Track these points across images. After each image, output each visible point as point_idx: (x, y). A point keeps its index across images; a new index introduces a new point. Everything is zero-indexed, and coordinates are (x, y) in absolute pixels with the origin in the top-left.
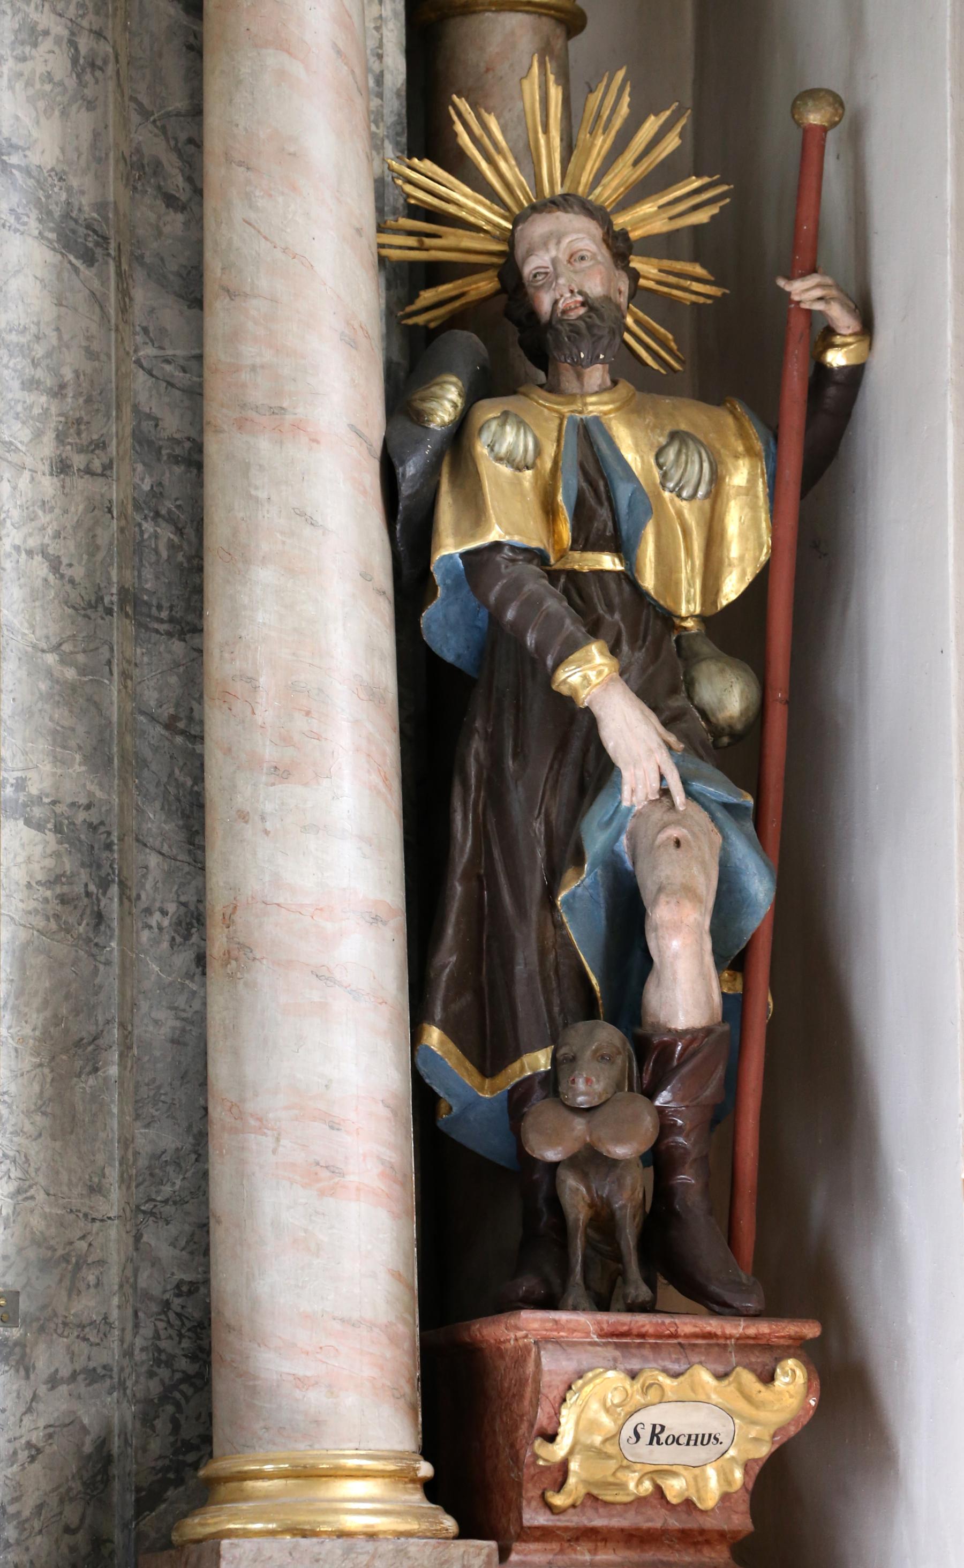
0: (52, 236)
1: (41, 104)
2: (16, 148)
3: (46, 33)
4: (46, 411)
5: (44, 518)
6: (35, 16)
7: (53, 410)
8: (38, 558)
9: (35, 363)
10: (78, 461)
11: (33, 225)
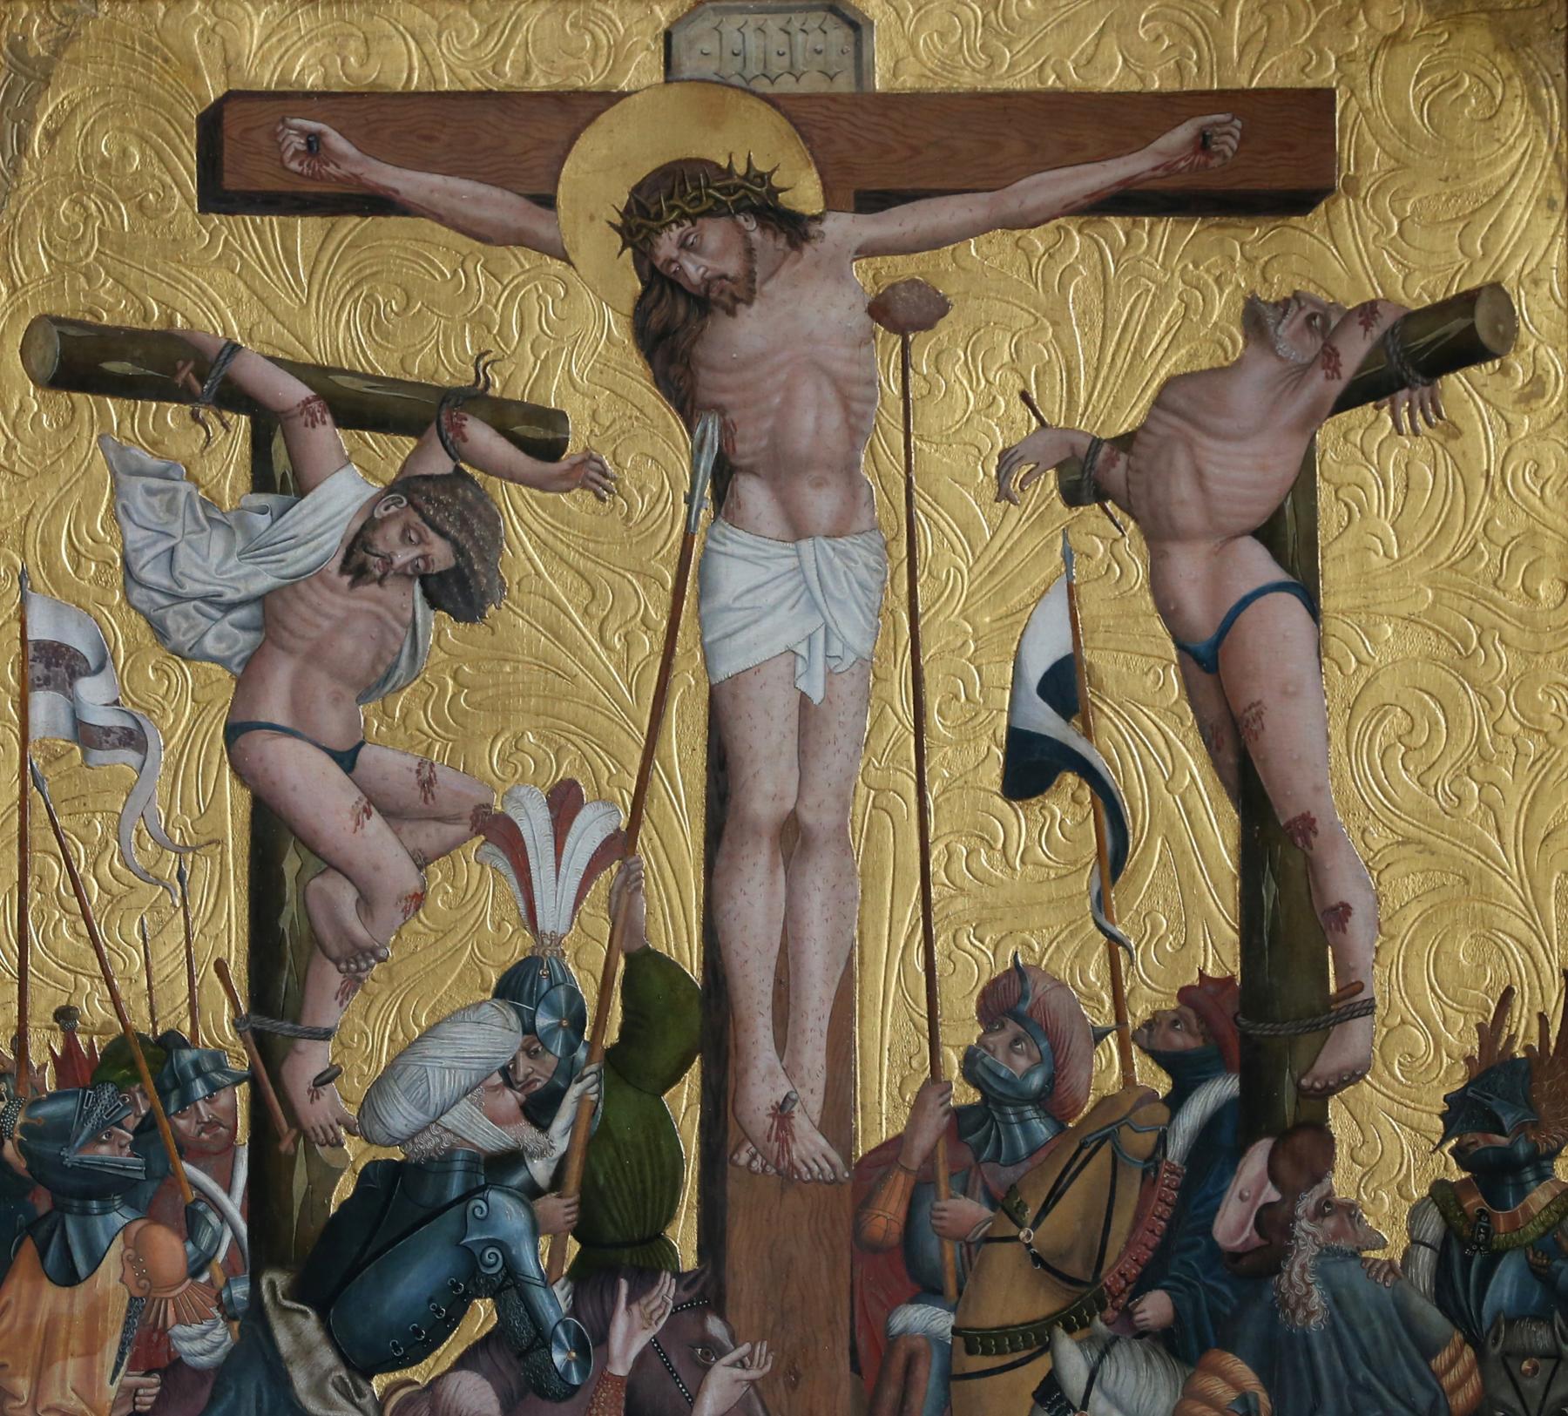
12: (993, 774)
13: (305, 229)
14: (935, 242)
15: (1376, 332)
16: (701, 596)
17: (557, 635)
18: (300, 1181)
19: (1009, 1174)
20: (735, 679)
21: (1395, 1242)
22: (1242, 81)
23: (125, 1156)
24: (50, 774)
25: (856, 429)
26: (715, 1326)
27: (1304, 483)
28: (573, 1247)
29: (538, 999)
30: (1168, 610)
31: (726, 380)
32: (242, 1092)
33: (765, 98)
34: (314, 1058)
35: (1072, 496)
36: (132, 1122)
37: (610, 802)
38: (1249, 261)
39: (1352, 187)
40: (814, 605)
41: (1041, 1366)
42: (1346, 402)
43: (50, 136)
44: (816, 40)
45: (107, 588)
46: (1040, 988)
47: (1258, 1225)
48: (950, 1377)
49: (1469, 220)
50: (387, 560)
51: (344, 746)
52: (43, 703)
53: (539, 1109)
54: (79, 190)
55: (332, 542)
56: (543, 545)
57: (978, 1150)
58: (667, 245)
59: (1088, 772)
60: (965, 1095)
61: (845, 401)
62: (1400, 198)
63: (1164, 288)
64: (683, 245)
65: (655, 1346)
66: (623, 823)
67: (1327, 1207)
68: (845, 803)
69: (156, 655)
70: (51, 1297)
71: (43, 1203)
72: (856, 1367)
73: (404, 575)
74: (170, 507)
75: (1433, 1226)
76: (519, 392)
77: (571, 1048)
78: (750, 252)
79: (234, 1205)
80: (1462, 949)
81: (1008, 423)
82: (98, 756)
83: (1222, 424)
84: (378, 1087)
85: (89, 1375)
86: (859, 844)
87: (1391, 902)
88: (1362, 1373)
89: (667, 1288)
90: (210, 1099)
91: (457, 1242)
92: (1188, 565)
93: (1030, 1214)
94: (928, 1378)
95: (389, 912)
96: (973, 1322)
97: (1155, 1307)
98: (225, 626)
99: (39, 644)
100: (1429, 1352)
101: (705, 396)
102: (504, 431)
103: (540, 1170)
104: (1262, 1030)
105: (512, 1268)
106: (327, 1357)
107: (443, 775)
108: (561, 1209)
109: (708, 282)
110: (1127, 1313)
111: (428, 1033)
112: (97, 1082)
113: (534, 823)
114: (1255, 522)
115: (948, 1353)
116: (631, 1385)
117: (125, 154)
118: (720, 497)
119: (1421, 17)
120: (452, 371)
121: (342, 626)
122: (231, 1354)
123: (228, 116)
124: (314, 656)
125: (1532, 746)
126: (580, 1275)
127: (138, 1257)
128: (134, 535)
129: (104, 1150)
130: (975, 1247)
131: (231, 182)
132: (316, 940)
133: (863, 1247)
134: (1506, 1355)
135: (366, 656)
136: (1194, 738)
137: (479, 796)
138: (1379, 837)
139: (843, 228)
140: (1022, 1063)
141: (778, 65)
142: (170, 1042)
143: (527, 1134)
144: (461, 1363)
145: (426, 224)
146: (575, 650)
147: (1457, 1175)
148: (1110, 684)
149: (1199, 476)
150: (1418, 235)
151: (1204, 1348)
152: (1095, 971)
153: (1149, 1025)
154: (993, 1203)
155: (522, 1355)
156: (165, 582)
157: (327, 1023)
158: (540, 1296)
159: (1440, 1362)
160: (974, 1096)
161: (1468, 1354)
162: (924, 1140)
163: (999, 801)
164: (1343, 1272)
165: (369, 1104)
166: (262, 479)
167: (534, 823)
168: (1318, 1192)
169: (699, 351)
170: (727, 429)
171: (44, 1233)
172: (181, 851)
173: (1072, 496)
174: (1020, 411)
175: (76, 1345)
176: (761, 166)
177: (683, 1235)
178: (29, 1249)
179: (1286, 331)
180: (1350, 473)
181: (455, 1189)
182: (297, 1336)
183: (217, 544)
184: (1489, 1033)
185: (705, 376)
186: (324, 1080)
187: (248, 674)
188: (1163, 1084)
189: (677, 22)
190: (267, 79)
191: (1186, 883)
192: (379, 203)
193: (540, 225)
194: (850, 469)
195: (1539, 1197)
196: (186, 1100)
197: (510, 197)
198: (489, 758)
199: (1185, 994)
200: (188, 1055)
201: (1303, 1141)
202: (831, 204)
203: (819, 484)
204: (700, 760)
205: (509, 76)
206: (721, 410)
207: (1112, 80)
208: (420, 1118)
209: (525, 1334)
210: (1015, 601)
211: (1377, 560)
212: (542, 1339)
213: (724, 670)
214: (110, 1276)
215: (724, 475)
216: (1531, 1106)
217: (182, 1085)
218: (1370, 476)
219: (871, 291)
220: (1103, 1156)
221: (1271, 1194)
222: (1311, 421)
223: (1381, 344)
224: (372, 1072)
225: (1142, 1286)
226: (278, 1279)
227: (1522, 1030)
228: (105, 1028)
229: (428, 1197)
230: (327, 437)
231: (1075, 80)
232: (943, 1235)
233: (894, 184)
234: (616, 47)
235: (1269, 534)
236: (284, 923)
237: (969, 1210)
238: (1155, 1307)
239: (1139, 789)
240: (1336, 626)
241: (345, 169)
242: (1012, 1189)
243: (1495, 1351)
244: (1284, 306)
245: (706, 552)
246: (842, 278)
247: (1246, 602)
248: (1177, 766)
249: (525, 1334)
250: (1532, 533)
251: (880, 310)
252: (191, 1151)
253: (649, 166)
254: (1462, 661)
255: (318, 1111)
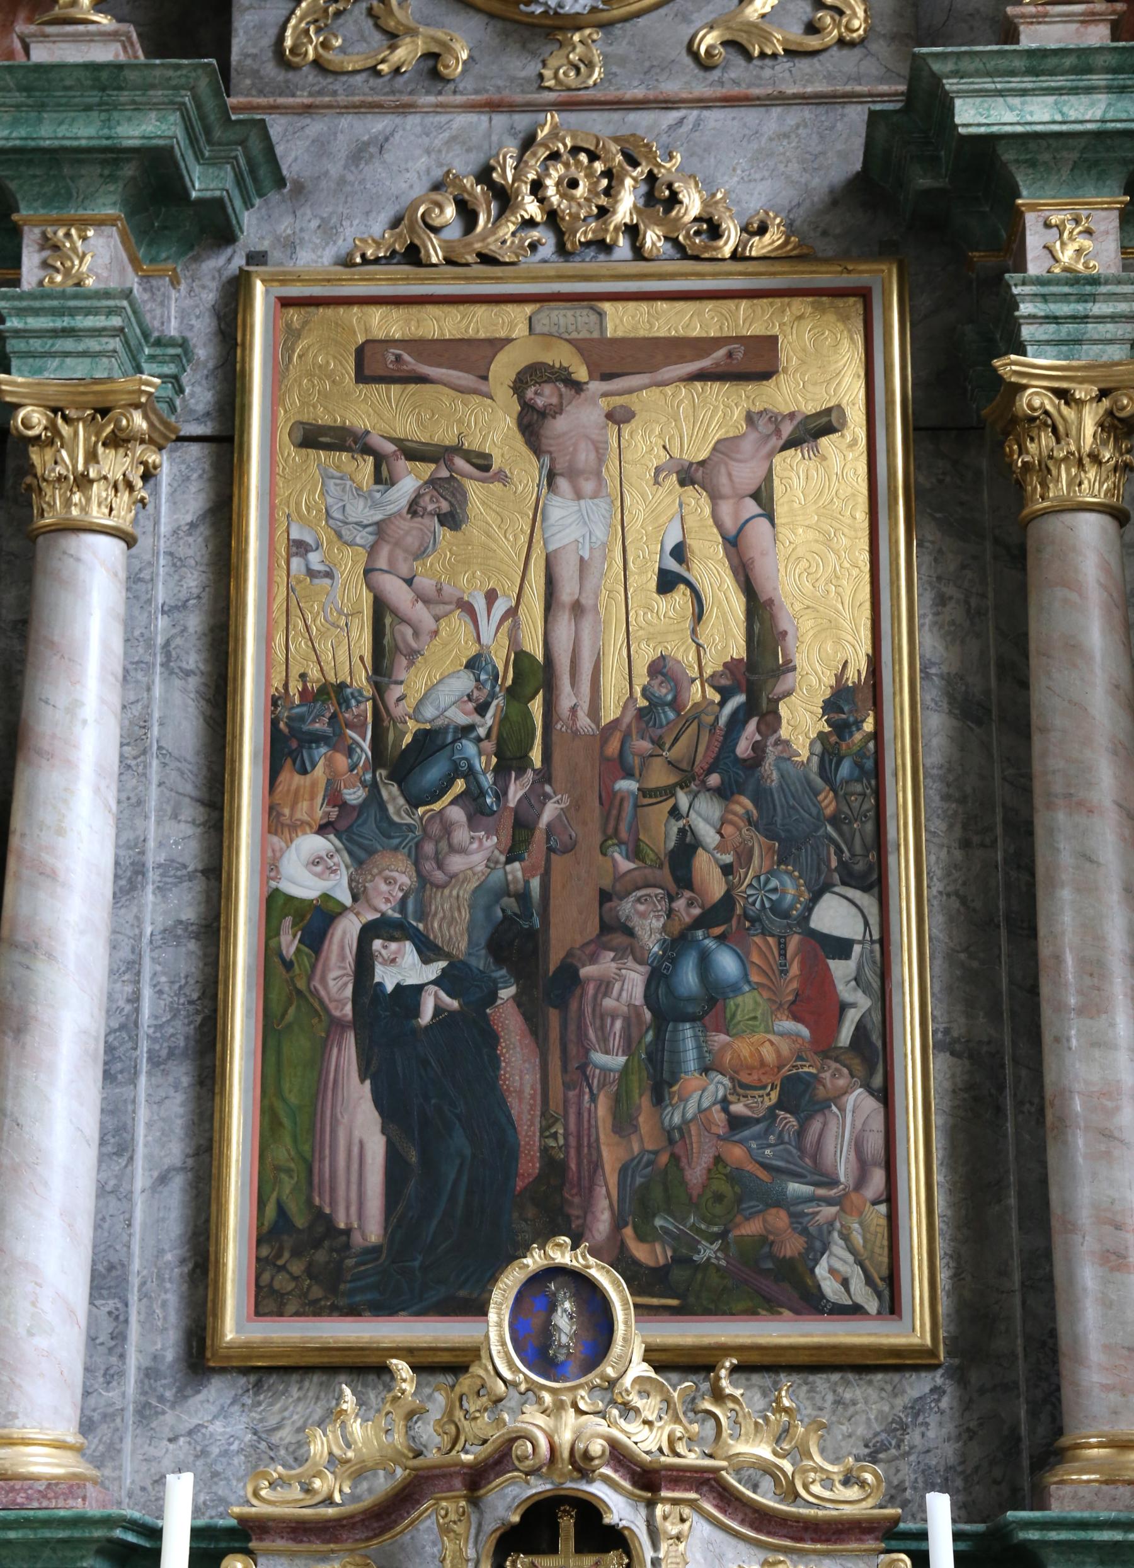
0: (957, 712)
1: (949, 638)
2: (934, 664)
3: (951, 598)
4: (956, 813)
5: (956, 874)
6: (944, 589)
7: (960, 811)
8: (953, 898)
9: (948, 785)
10: (976, 839)
11: (945, 706)
12: (653, 584)
13: (395, 389)
14: (630, 391)
15: (795, 422)
16: (543, 520)
17: (488, 536)
18: (391, 736)
19: (659, 732)
20: (555, 551)
21: (804, 754)
22: (744, 333)
23: (325, 727)
24: (298, 588)
25: (601, 459)
26: (548, 788)
27: (769, 478)
28: (494, 760)
29: (481, 669)
30: (718, 524)
31: (552, 442)
32: (369, 704)
33: (566, 340)
34: (396, 691)
35: (682, 483)
36: (328, 715)
37: (509, 596)
38: (748, 397)
39: (785, 370)
40: (585, 523)
41: (671, 802)
42: (784, 448)
43: (300, 357)
44: (585, 319)
45: (320, 520)
46: (670, 664)
47: (753, 749)
48: (637, 806)
49: (828, 382)
50: (425, 509)
51: (408, 577)
52: (296, 562)
53: (482, 709)
54: (310, 375)
55: (404, 502)
56: (483, 503)
57: (647, 723)
58: (530, 393)
59: (689, 584)
60: (642, 703)
61: (597, 450)
62: (803, 374)
63: (716, 408)
64: (536, 393)
65: (525, 796)
66: (513, 603)
67: (779, 742)
68: (597, 596)
69: (338, 544)
70: (298, 779)
71: (294, 744)
72: (601, 803)
73: (430, 514)
74: (344, 490)
75: (818, 748)
76: (475, 447)
77: (493, 687)
78: (561, 396)
79: (366, 745)
80: (829, 647)
81: (657, 457)
82: (316, 581)
83: (738, 456)
84: (421, 702)
85: (312, 808)
86: (602, 611)
87: (802, 630)
88: (792, 802)
89: (530, 774)
90: (357, 706)
91: (450, 758)
92: (726, 509)
93: (667, 746)
94: (628, 807)
95: (425, 638)
96: (645, 786)
97: (714, 780)
98: (364, 533)
99: (294, 541)
100: (816, 794)
101: (544, 448)
102: (469, 461)
103: (482, 732)
104: (754, 678)
105: (471, 768)
106: (401, 801)
107: (445, 587)
108: (489, 746)
109: (545, 407)
110: (703, 782)
111: (440, 681)
112: (315, 701)
113: (480, 605)
114: (751, 492)
115: (636, 798)
116: (516, 811)
117: (328, 363)
118: (550, 484)
119: (809, 310)
120: (450, 440)
121: (407, 533)
122: (365, 800)
123: (367, 348)
124: (397, 544)
125: (855, 572)
126: (497, 770)
127: (330, 763)
128: (330, 500)
129: (317, 725)
130: (646, 759)
131: (367, 372)
132: (397, 648)
133: (604, 759)
134: (846, 794)
135: (417, 544)
136: (729, 571)
137: (458, 594)
138: (798, 606)
139: (596, 386)
140: (664, 691)
141: (571, 328)
142: (342, 686)
143: (477, 719)
144: (452, 803)
145: (440, 387)
146: (495, 541)
147: (827, 729)
148: (697, 552)
149: (730, 475)
150: (810, 388)
151: (732, 794)
152: (692, 656)
153: (712, 676)
154: (653, 742)
155: (475, 800)
156: (340, 517)
157: (401, 678)
158: (482, 778)
159: (820, 798)
160: (646, 703)
161: (831, 794)
162: (627, 720)
163: (655, 595)
164: (783, 765)
165: (417, 708)
166: (378, 479)
167: (480, 605)
168: (775, 736)
169: (542, 432)
170: (552, 460)
171: (295, 755)
172: (347, 616)
173: (682, 483)
174: (662, 452)
175: (307, 796)
176: (565, 364)
177: (536, 755)
178: (289, 761)
179: (762, 423)
180: (786, 474)
181: (450, 738)
182: (390, 793)
183: (361, 503)
184: (839, 678)
185: (544, 441)
186: (400, 699)
187: (372, 551)
188: (717, 698)
189: (533, 313)
190: (381, 335)
191: (726, 623)
192: (423, 379)
193: (482, 386)
194: (598, 474)
195: (858, 736)
196: (348, 707)
197: (471, 377)
198: (463, 580)
199: (725, 665)
200: (349, 691)
201: (770, 718)
202: (591, 378)
203: (587, 479)
204: (542, 580)
205: (471, 333)
206: (550, 453)
207: (696, 332)
208: (436, 713)
209: (476, 792)
210: (661, 521)
211: (796, 505)
212: (483, 794)
213: (551, 548)
214: (319, 772)
215: (551, 477)
216: (854, 703)
217: (347, 701)
218: (793, 475)
219: (606, 409)
220: (695, 725)
221: (758, 737)
222: (771, 455)
223: (797, 427)
224: (418, 696)
225: (709, 772)
226: (382, 773)
227: (851, 676)
228: (318, 681)
229: (439, 742)
230: (402, 464)
231: (682, 333)
232: (634, 754)
233: (615, 370)
234: (511, 322)
235: (756, 496)
236: (385, 642)
237: (645, 745)
238: (714, 780)
239: (708, 590)
240: (783, 531)
241: (410, 367)
242: (661, 737)
243: (841, 793)
244: (761, 413)
245: (545, 505)
246: (596, 404)
247: (747, 521)
248: (722, 582)
249: (476, 792)
250: (853, 495)
251: (610, 416)
252: (349, 725)
253: (523, 365)
254: (828, 541)
255: (398, 711)
